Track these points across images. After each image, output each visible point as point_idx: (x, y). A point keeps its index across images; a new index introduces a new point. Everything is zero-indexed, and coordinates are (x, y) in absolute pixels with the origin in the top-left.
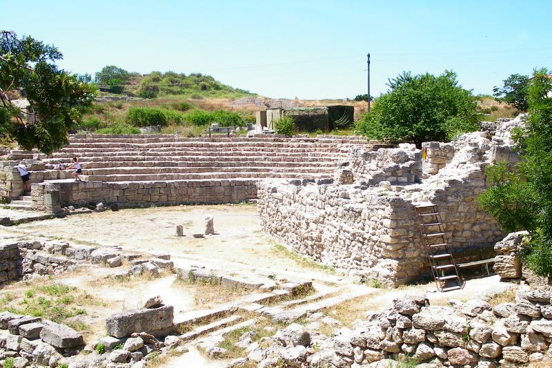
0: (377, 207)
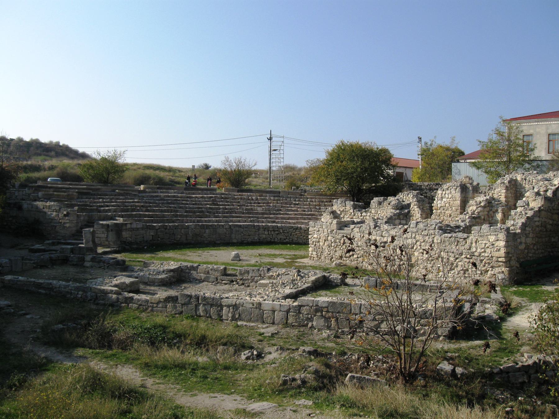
0: (487, 234)
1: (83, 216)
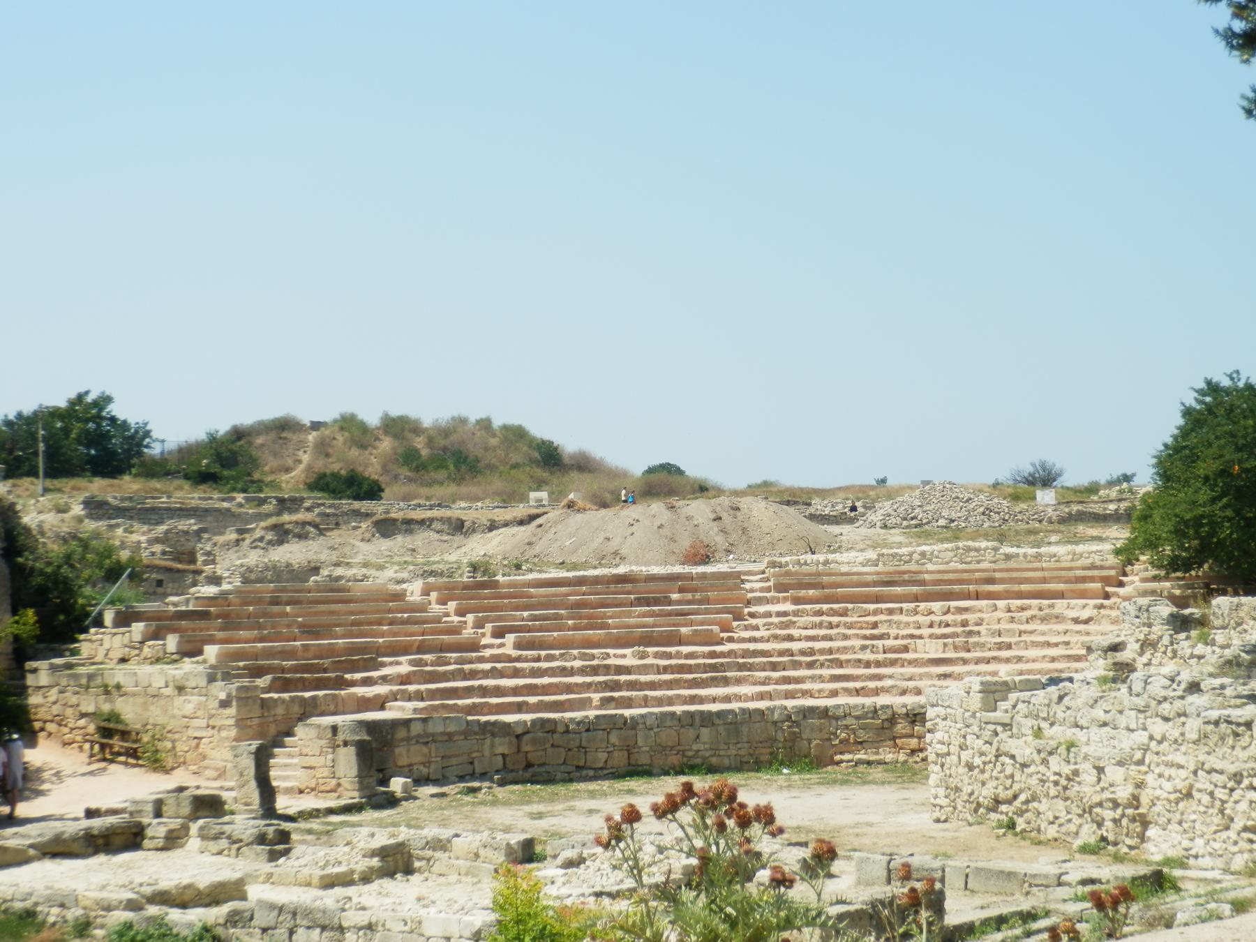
1: (283, 701)
